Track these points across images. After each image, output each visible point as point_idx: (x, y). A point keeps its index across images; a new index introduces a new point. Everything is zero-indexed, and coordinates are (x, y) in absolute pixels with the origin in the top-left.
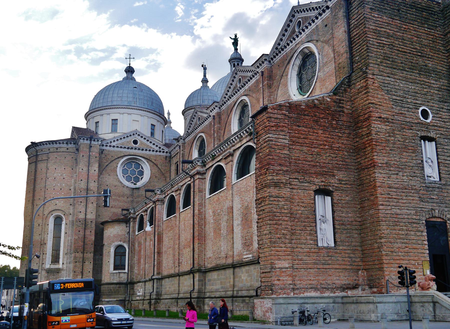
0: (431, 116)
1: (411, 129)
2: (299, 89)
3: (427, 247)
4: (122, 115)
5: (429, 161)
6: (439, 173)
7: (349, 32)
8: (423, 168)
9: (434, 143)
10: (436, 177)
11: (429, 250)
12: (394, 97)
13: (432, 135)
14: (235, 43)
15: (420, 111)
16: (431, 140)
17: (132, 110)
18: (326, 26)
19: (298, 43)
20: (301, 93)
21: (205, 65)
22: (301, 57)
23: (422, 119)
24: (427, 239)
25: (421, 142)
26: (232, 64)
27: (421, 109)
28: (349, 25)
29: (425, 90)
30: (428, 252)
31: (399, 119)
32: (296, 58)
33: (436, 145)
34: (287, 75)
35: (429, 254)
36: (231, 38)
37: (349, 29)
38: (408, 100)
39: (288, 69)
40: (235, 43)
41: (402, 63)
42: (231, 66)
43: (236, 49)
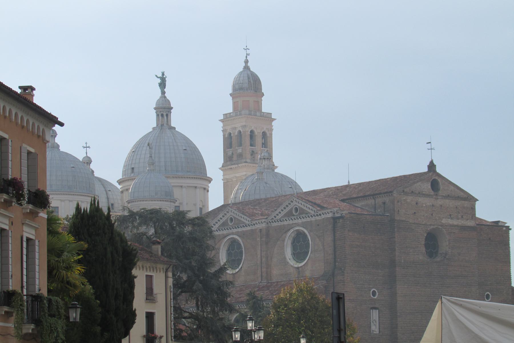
0: (377, 294)
1: (366, 304)
2: (293, 255)
4: (63, 203)
5: (374, 322)
6: (379, 329)
7: (334, 241)
8: (370, 327)
9: (377, 311)
10: (377, 331)
12: (358, 286)
13: (377, 306)
14: (162, 85)
15: (371, 292)
16: (375, 308)
17: (72, 196)
18: (318, 225)
19: (295, 223)
20: (294, 258)
21: (151, 144)
22: (296, 233)
23: (372, 296)
25: (370, 311)
26: (160, 114)
27: (372, 290)
28: (334, 236)
29: (376, 278)
31: (360, 299)
32: (292, 232)
33: (379, 312)
34: (284, 241)
36: (156, 76)
37: (334, 239)
38: (365, 286)
39: (285, 237)
40: (163, 85)
41: (363, 263)
42: (158, 115)
43: (163, 93)
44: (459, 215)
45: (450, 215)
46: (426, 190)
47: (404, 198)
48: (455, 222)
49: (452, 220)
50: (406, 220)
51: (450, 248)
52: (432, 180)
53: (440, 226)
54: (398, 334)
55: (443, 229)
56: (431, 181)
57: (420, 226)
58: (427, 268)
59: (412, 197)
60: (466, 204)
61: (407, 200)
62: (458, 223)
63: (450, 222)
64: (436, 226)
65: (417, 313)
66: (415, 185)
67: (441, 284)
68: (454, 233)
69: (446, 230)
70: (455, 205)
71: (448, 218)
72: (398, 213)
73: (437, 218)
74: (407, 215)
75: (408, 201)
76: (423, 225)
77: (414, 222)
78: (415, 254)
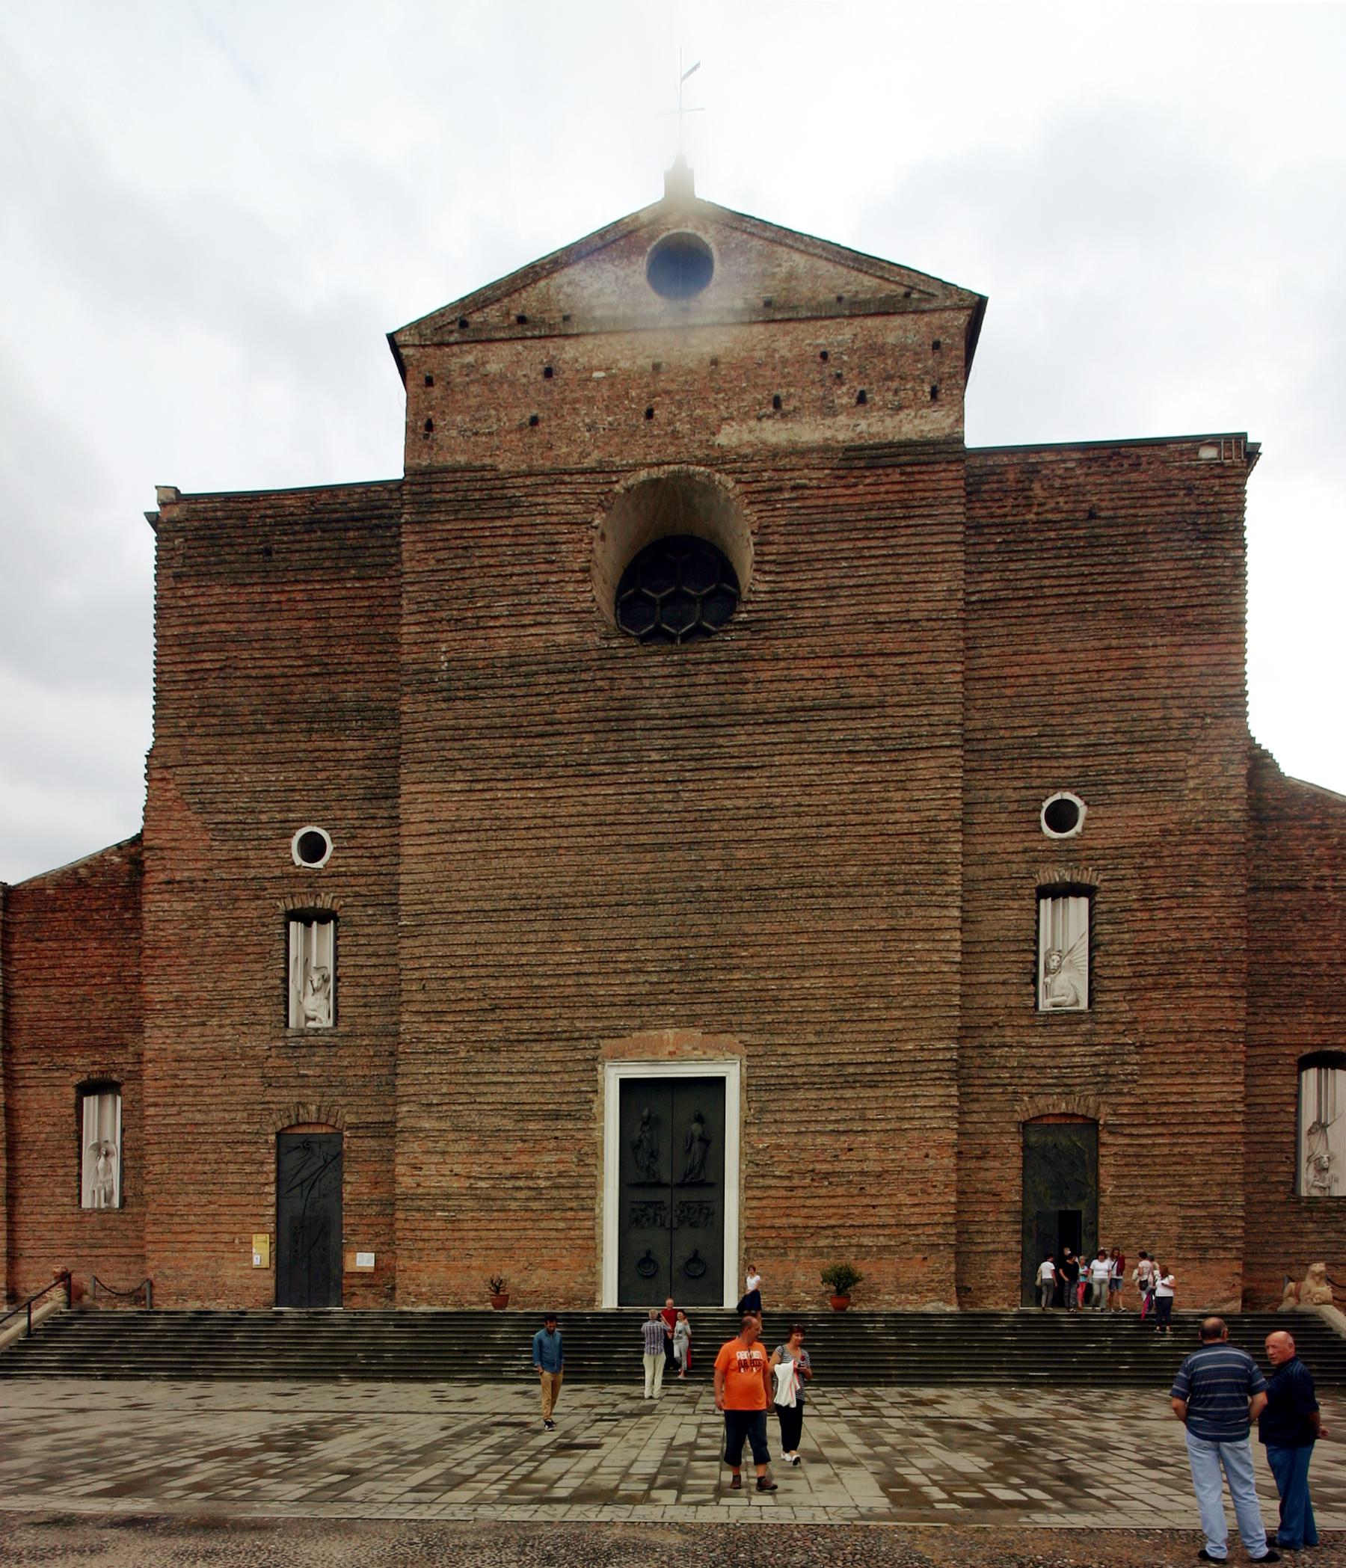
3: (272, 1199)
11: (278, 1205)
24: (272, 1177)
30: (272, 1211)
35: (278, 1215)
44: (844, 389)
45: (777, 402)
46: (614, 299)
47: (470, 359)
48: (809, 432)
49: (790, 425)
50: (477, 463)
51: (767, 568)
52: (654, 243)
53: (698, 464)
54: (406, 1017)
55: (717, 476)
56: (649, 249)
57: (563, 483)
58: (600, 683)
59: (520, 348)
60: (894, 331)
61: (488, 366)
62: (828, 434)
63: (775, 433)
64: (672, 468)
65: (523, 909)
66: (542, 283)
67: (692, 759)
68: (794, 488)
69: (738, 482)
70: (818, 346)
71: (759, 419)
72: (426, 437)
73: (683, 428)
74: (484, 439)
75: (493, 368)
76: (583, 472)
77: (524, 467)
78: (526, 621)
